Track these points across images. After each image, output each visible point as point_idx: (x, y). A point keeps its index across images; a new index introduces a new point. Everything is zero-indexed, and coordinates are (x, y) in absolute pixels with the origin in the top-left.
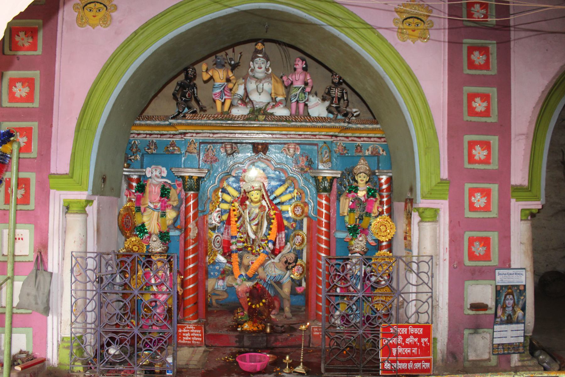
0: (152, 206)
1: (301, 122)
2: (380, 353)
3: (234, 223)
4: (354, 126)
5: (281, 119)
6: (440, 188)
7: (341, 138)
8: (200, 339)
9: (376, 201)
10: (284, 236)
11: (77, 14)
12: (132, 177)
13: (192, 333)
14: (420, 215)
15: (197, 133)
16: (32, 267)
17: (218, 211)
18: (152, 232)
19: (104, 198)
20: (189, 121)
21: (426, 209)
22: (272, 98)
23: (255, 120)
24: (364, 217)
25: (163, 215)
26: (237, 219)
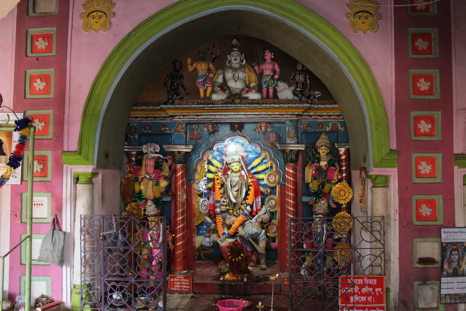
0: (148, 177)
1: (271, 104)
2: (340, 300)
3: (218, 189)
4: (316, 106)
5: (254, 102)
6: (390, 158)
7: (305, 117)
8: (189, 287)
9: (336, 170)
10: (260, 200)
11: (82, 21)
12: (131, 153)
13: (182, 282)
14: (372, 181)
15: (184, 116)
16: (50, 227)
17: (205, 180)
18: (148, 198)
19: (108, 171)
20: (177, 106)
21: (377, 176)
22: (246, 85)
23: (231, 104)
24: (326, 184)
25: (157, 184)
26: (220, 186)
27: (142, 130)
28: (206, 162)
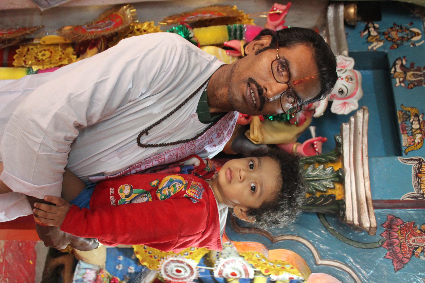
17: (246, 271)
27: (400, 58)
28: (295, 277)
